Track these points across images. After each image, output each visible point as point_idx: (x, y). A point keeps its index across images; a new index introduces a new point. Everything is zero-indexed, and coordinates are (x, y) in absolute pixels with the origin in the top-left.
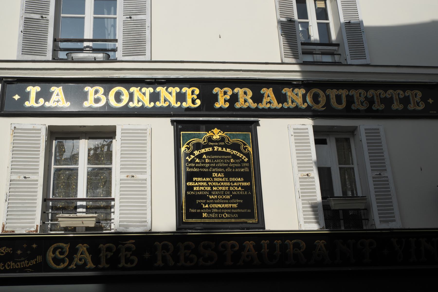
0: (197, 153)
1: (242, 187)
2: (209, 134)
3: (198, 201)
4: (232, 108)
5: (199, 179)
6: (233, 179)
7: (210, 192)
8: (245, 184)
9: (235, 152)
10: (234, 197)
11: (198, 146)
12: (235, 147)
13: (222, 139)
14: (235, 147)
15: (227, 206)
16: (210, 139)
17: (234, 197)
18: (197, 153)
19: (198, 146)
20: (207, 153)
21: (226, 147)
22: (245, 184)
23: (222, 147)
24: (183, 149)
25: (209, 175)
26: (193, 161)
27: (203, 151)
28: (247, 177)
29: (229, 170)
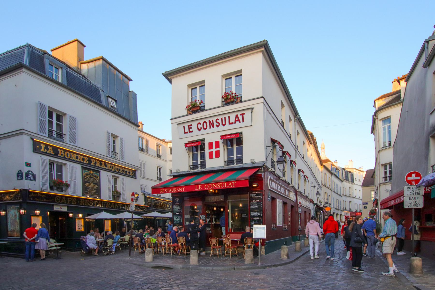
0: (87, 176)
1: (97, 187)
2: (90, 172)
3: (87, 189)
4: (95, 166)
5: (88, 184)
6: (95, 185)
7: (90, 187)
8: (97, 187)
9: (95, 178)
10: (95, 189)
11: (87, 175)
12: (95, 176)
13: (93, 174)
14: (95, 176)
15: (93, 191)
16: (90, 173)
17: (95, 189)
18: (87, 176)
19: (87, 175)
20: (90, 177)
21: (94, 176)
22: (97, 187)
23: (93, 176)
24: (84, 175)
25: (89, 183)
26: (86, 178)
27: (88, 176)
28: (97, 185)
29: (94, 182)
